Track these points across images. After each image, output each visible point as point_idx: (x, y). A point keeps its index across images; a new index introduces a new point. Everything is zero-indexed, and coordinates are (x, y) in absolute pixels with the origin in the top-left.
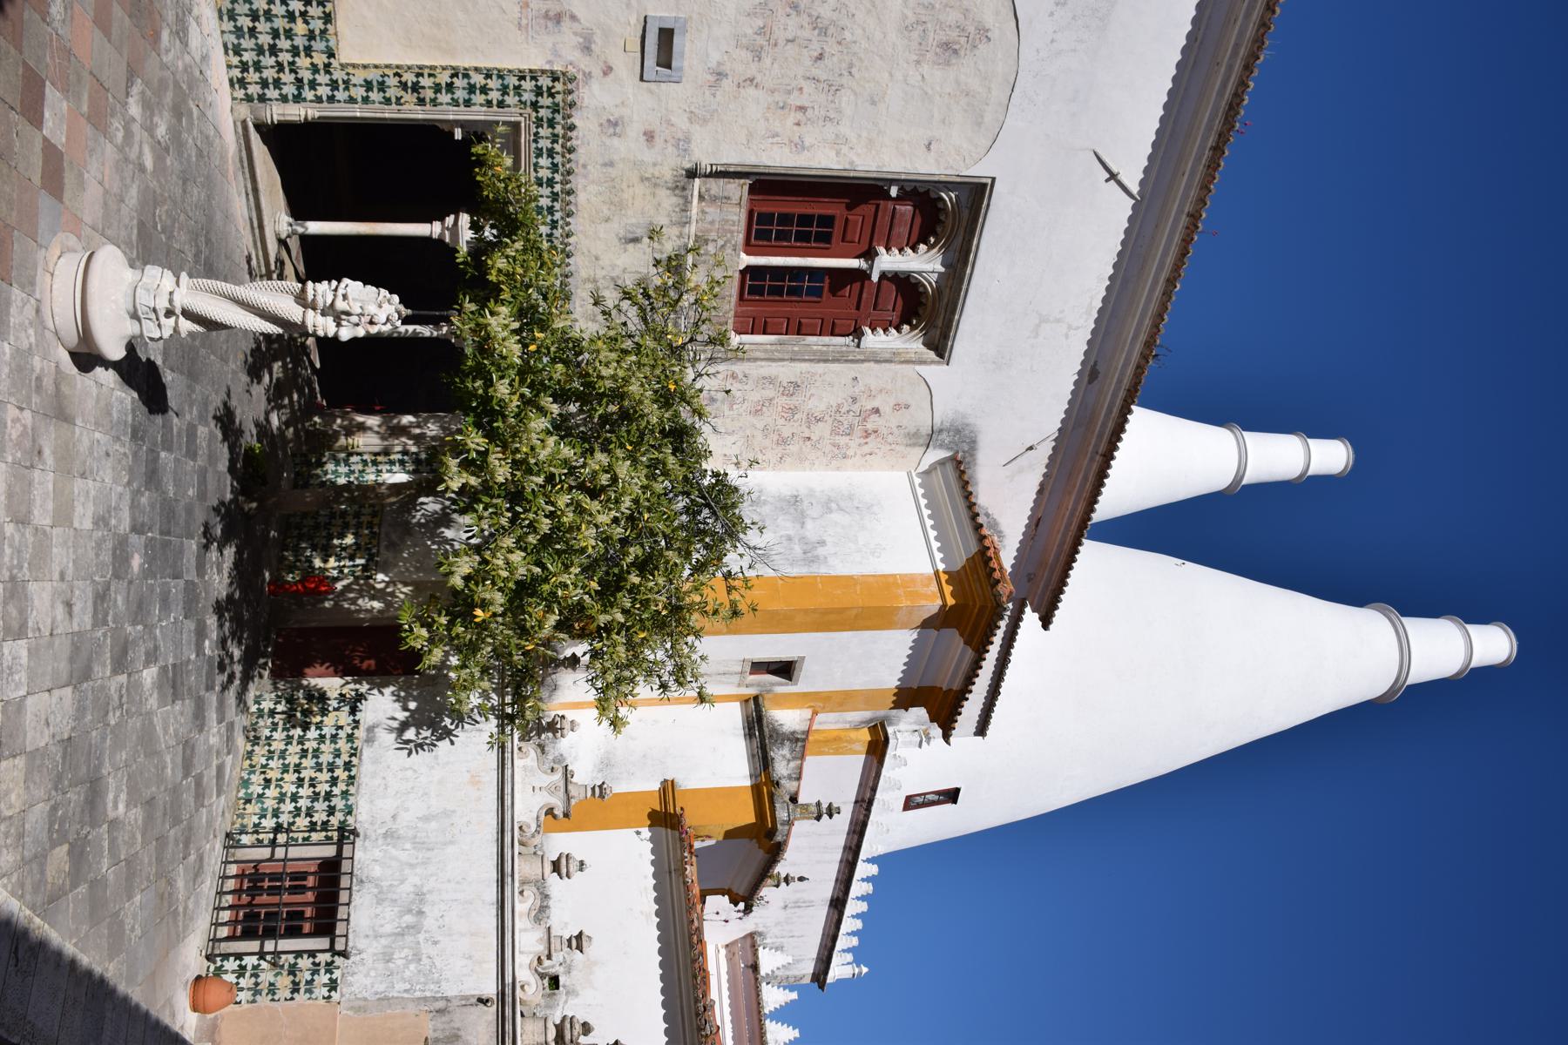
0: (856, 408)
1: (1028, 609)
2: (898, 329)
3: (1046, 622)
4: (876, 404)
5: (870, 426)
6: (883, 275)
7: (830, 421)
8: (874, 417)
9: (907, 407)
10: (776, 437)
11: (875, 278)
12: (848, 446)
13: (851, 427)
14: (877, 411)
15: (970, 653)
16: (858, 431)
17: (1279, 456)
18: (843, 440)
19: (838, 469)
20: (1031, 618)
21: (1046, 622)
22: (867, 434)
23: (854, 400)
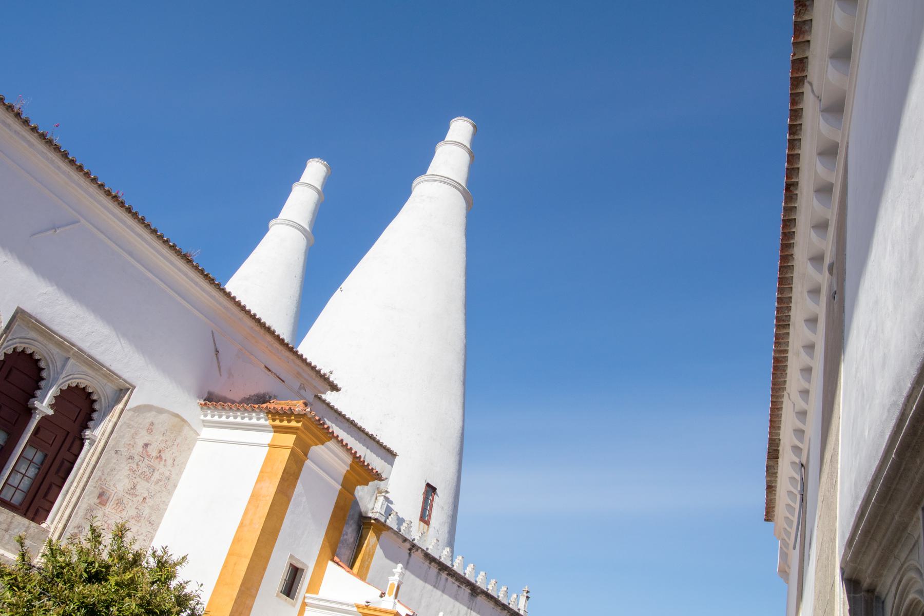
0: (137, 458)
1: (324, 396)
2: (94, 411)
3: (334, 388)
4: (140, 443)
5: (154, 454)
6: (52, 406)
7: (138, 479)
8: (149, 449)
9: (152, 424)
10: (133, 521)
11: (51, 412)
12: (163, 474)
13: (149, 467)
14: (146, 445)
15: (331, 444)
16: (155, 463)
17: (301, 202)
18: (156, 476)
19: (175, 486)
20: (329, 397)
21: (334, 388)
22: (159, 458)
23: (131, 458)
